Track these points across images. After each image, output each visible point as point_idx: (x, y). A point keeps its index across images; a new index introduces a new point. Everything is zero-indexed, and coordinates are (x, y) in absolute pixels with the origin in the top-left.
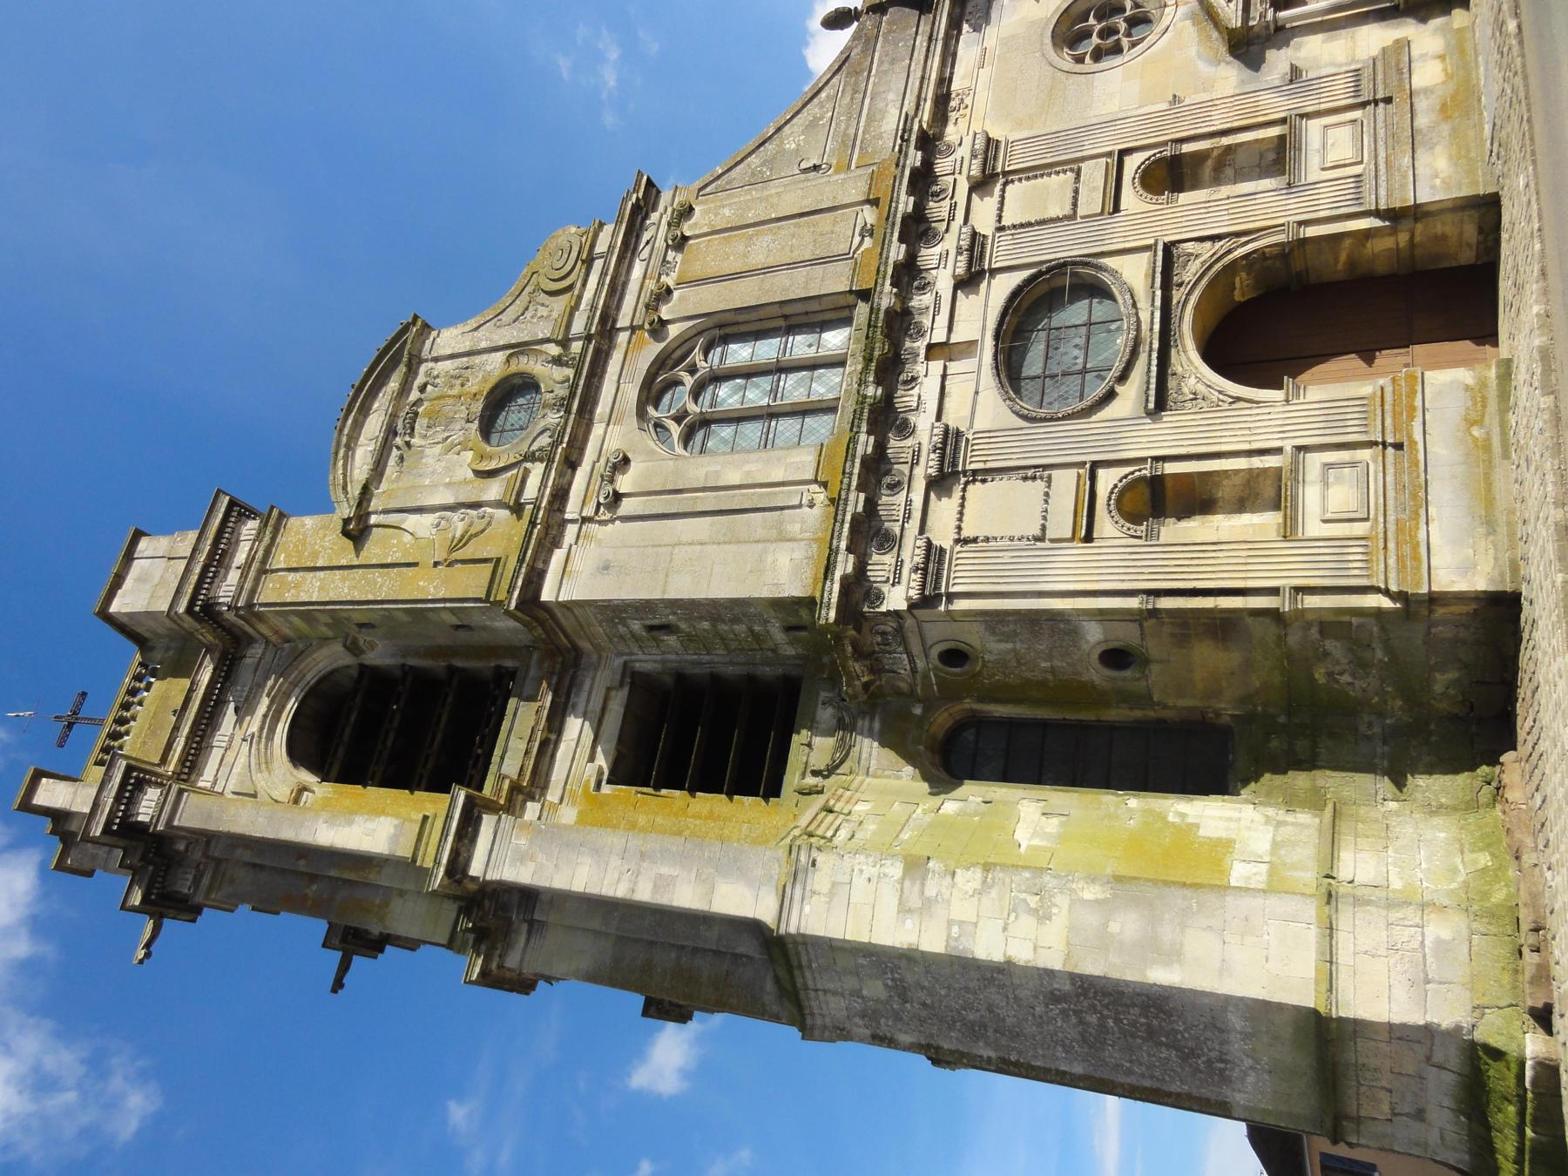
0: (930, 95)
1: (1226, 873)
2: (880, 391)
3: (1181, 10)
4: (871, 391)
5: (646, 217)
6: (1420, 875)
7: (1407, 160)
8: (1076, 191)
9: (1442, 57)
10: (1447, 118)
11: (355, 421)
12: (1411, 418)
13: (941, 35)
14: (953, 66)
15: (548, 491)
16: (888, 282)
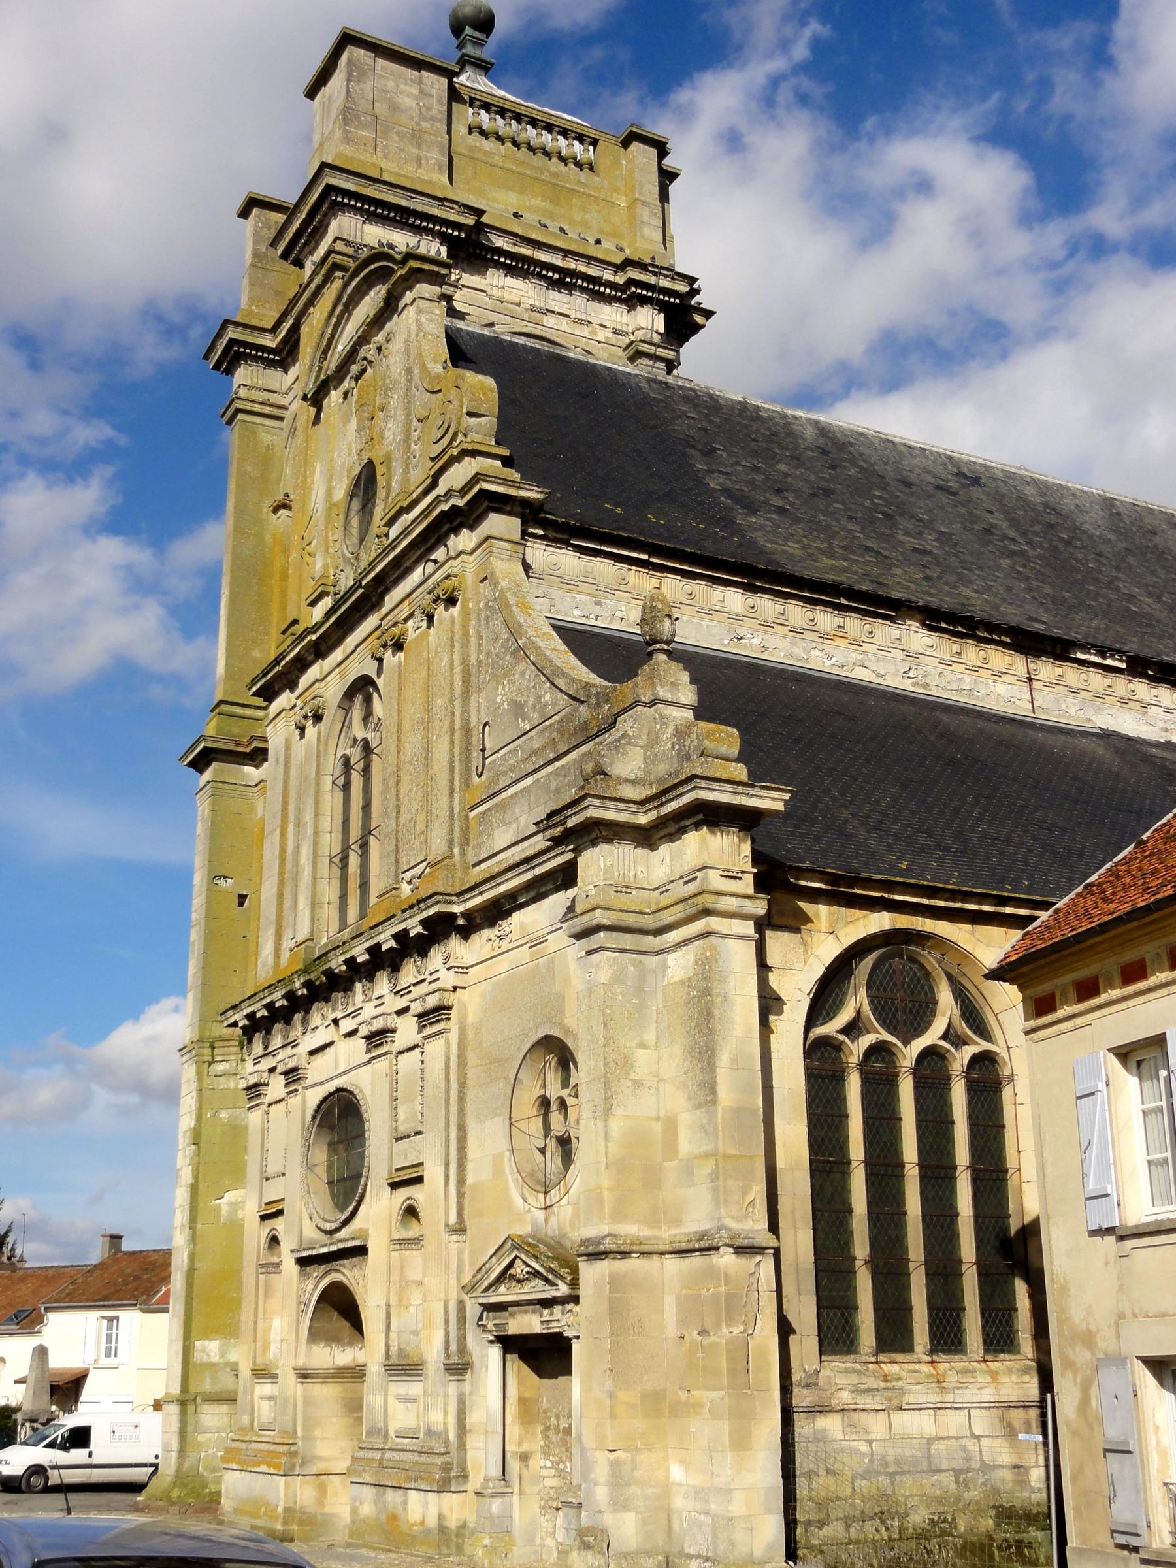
0: (488, 896)
1: (207, 1335)
2: (300, 993)
3: (541, 1214)
4: (298, 984)
5: (456, 531)
6: (210, 1451)
7: (367, 1479)
8: (409, 1136)
9: (423, 1523)
10: (388, 1518)
11: (358, 287)
12: (269, 1466)
13: (539, 871)
14: (535, 900)
15: (292, 655)
16: (342, 958)
